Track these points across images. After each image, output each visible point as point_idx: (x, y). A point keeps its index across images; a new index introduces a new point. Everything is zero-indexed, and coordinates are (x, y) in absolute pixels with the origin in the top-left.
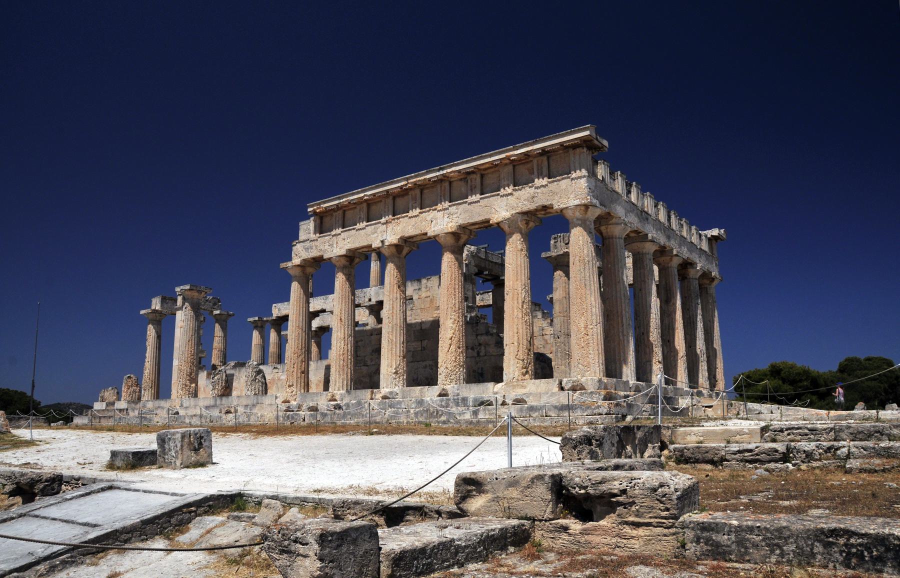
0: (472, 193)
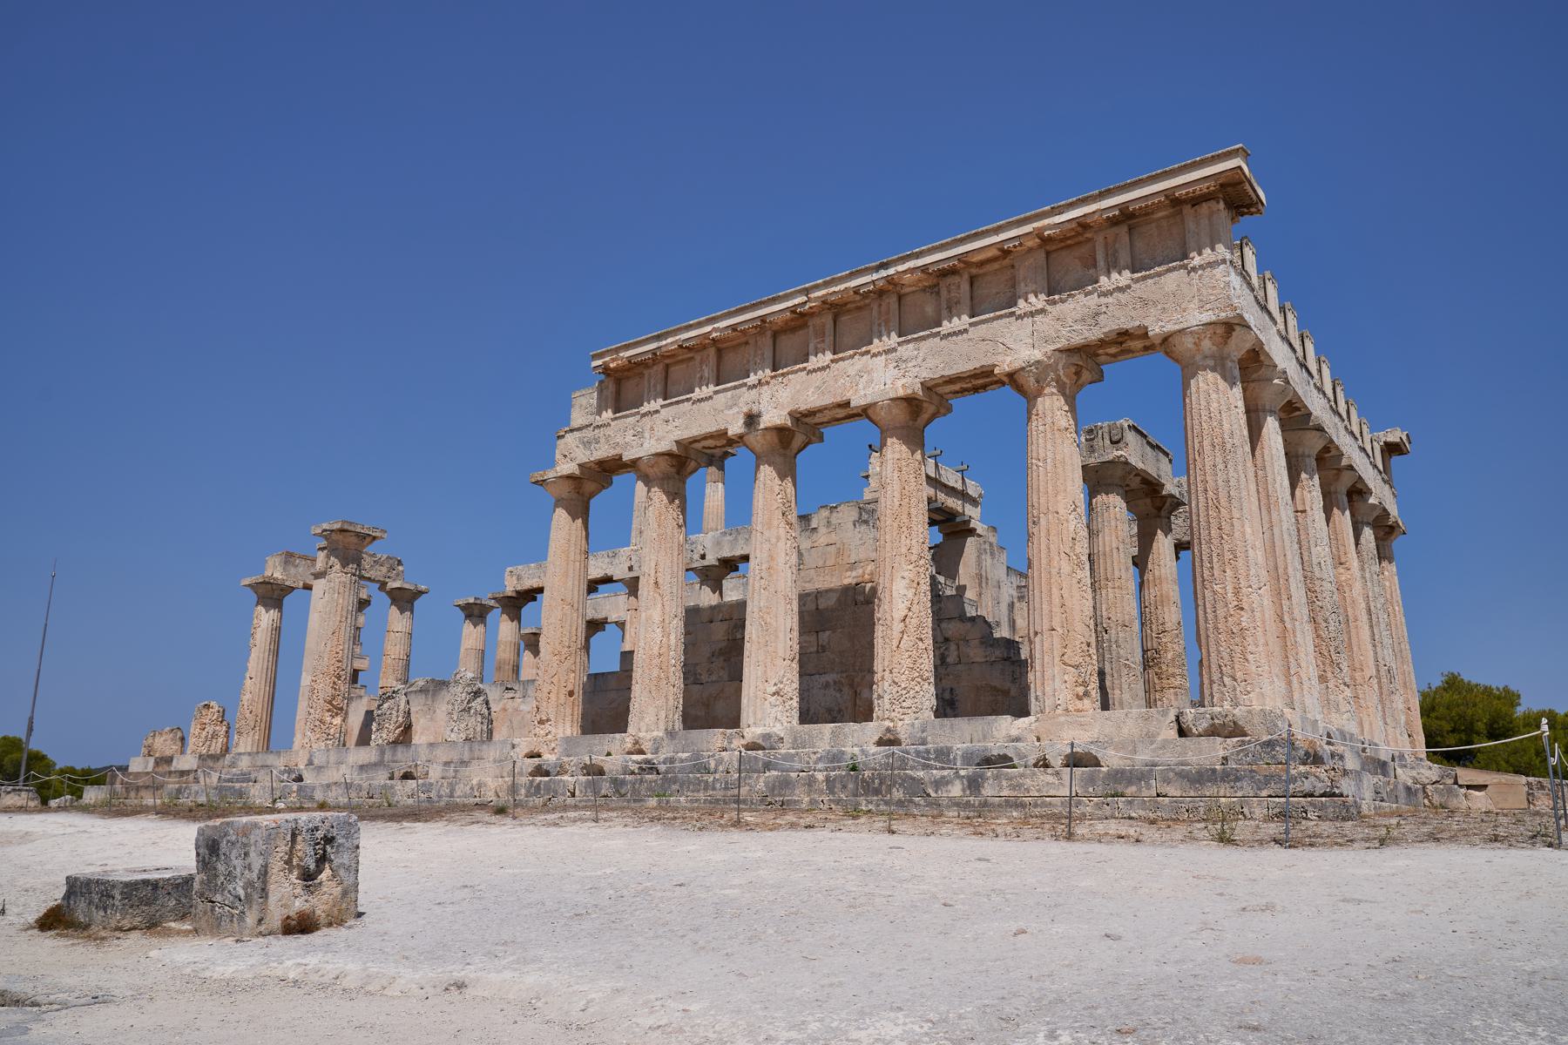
0: (952, 310)
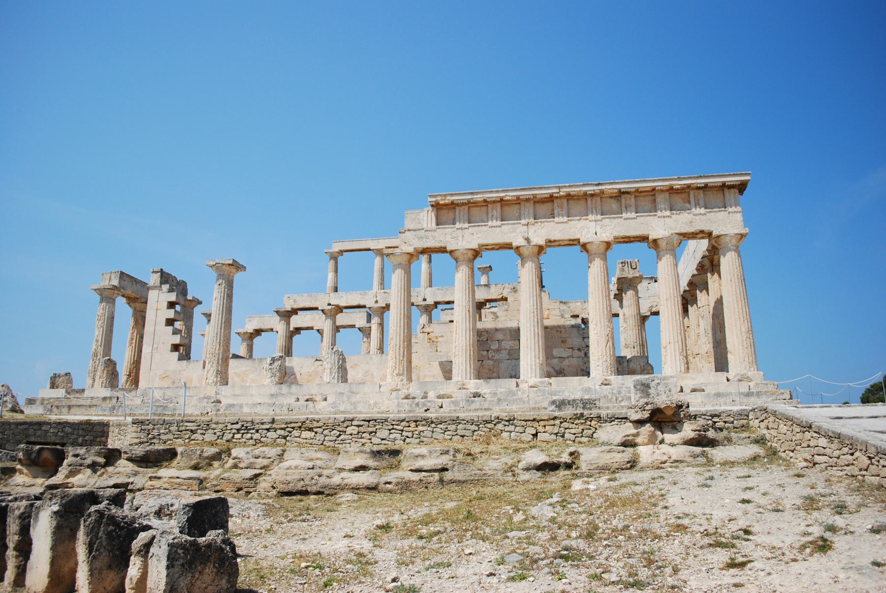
0: (627, 208)
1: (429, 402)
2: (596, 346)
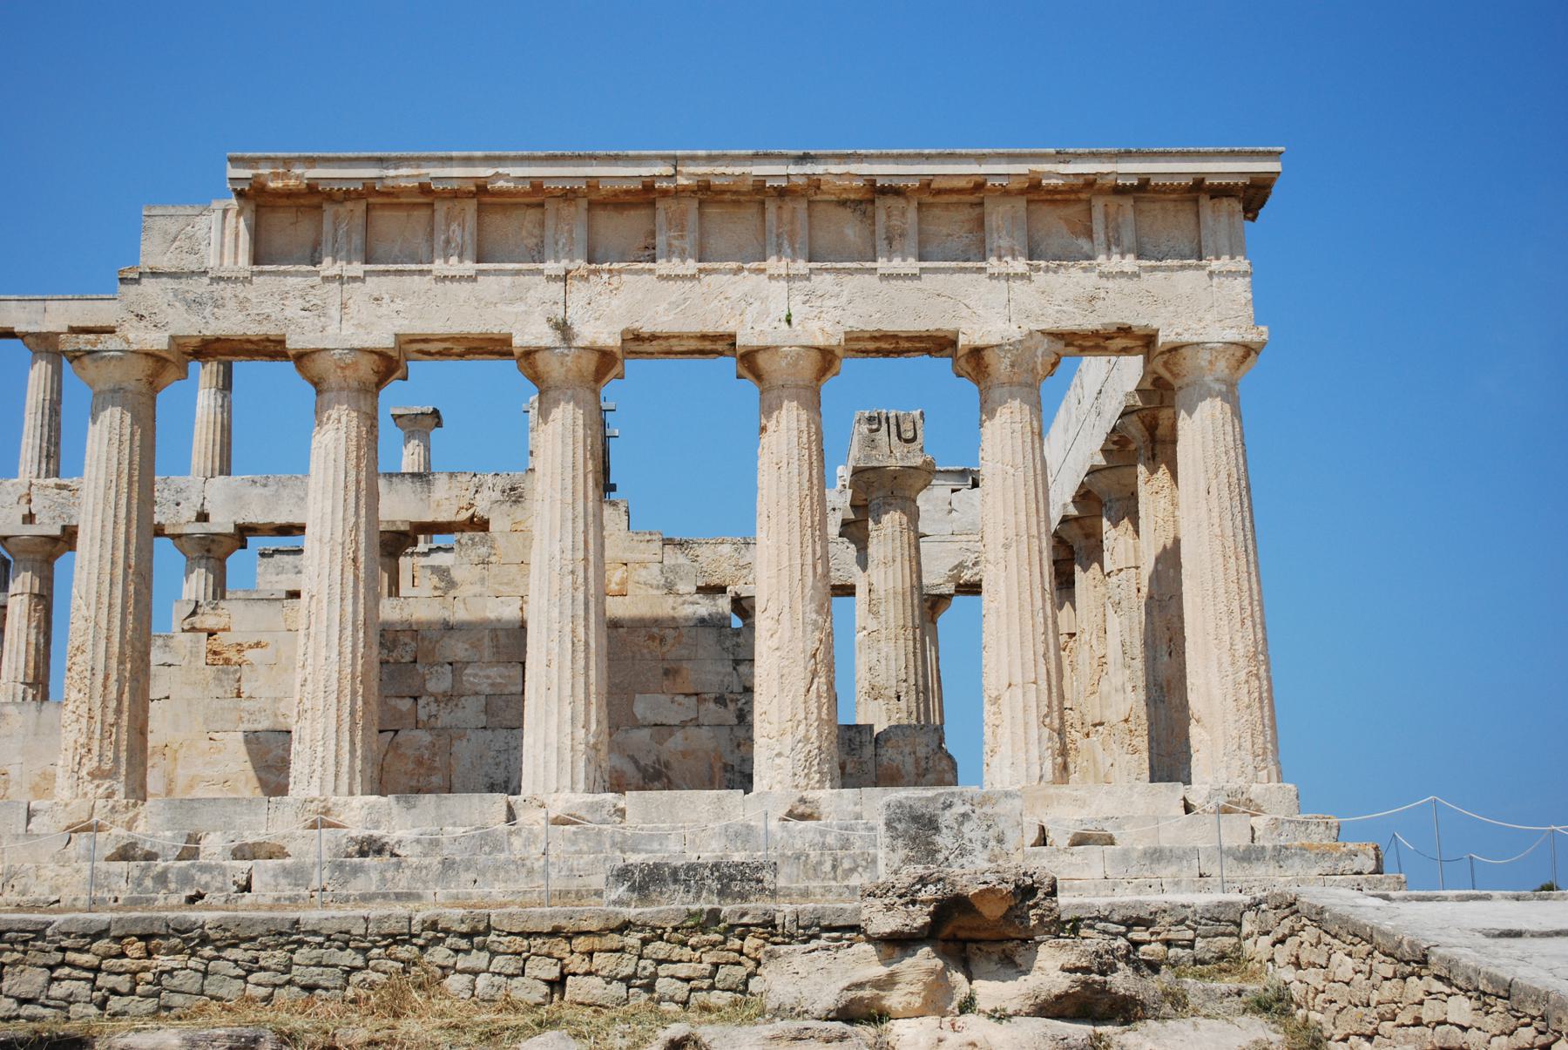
0: (893, 242)
1: (204, 869)
2: (775, 691)
